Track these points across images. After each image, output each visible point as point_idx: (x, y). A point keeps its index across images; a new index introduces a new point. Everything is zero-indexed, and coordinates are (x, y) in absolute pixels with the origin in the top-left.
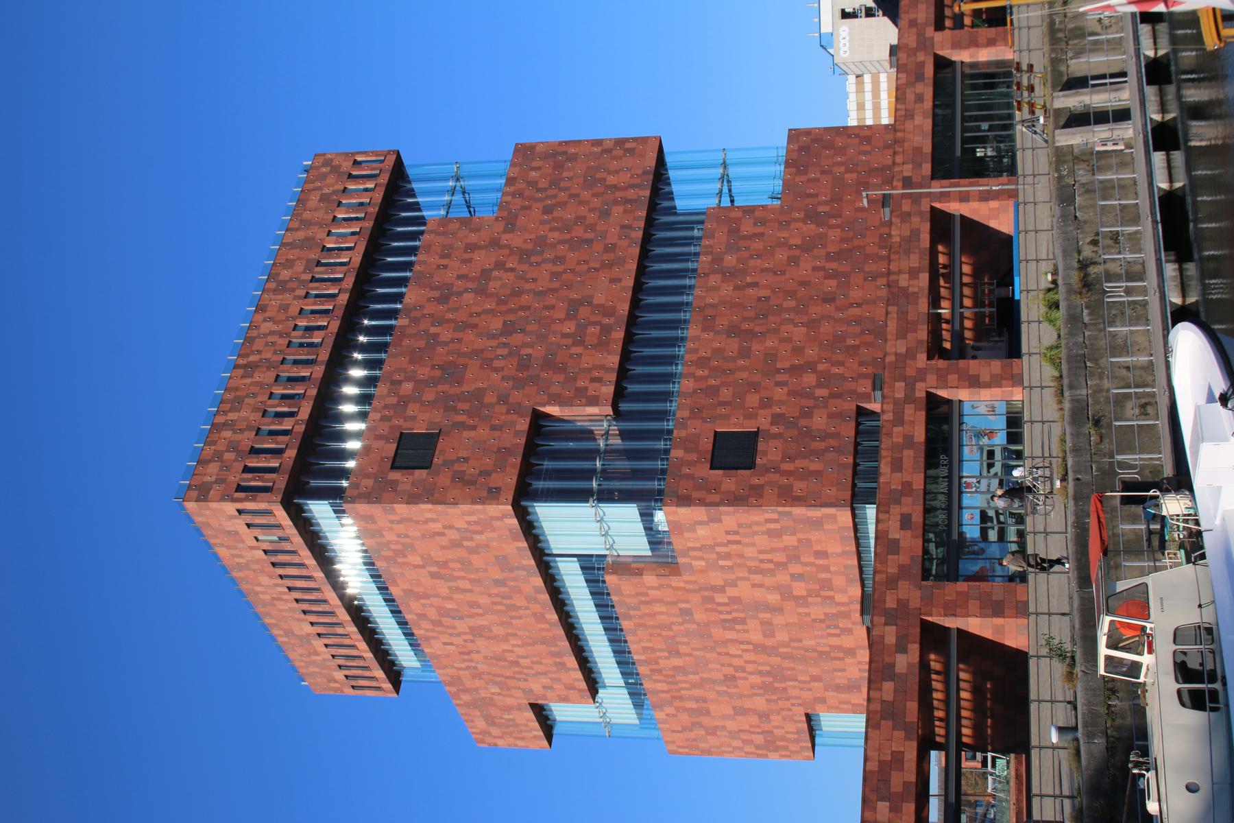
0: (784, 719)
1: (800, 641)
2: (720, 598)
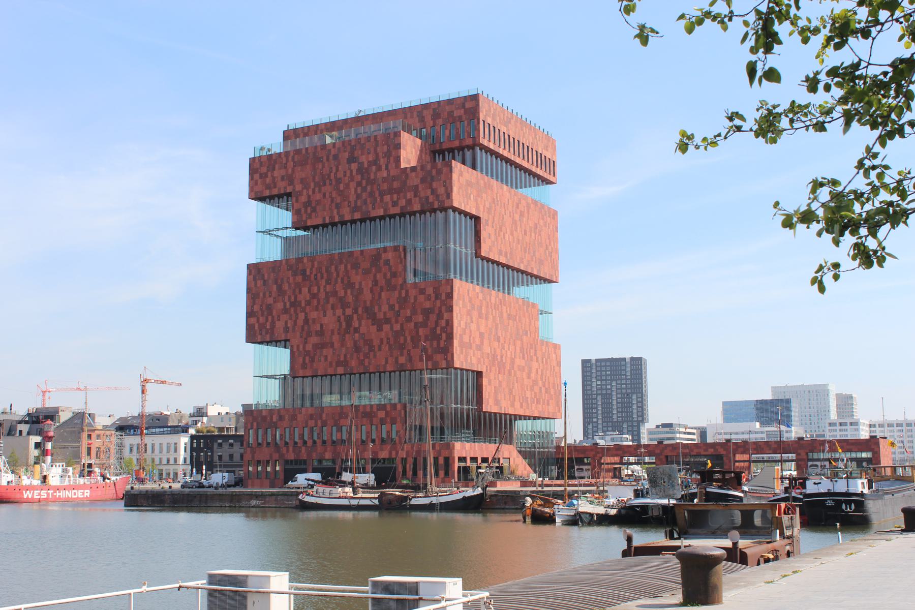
0: (479, 359)
1: (517, 382)
2: (532, 351)
